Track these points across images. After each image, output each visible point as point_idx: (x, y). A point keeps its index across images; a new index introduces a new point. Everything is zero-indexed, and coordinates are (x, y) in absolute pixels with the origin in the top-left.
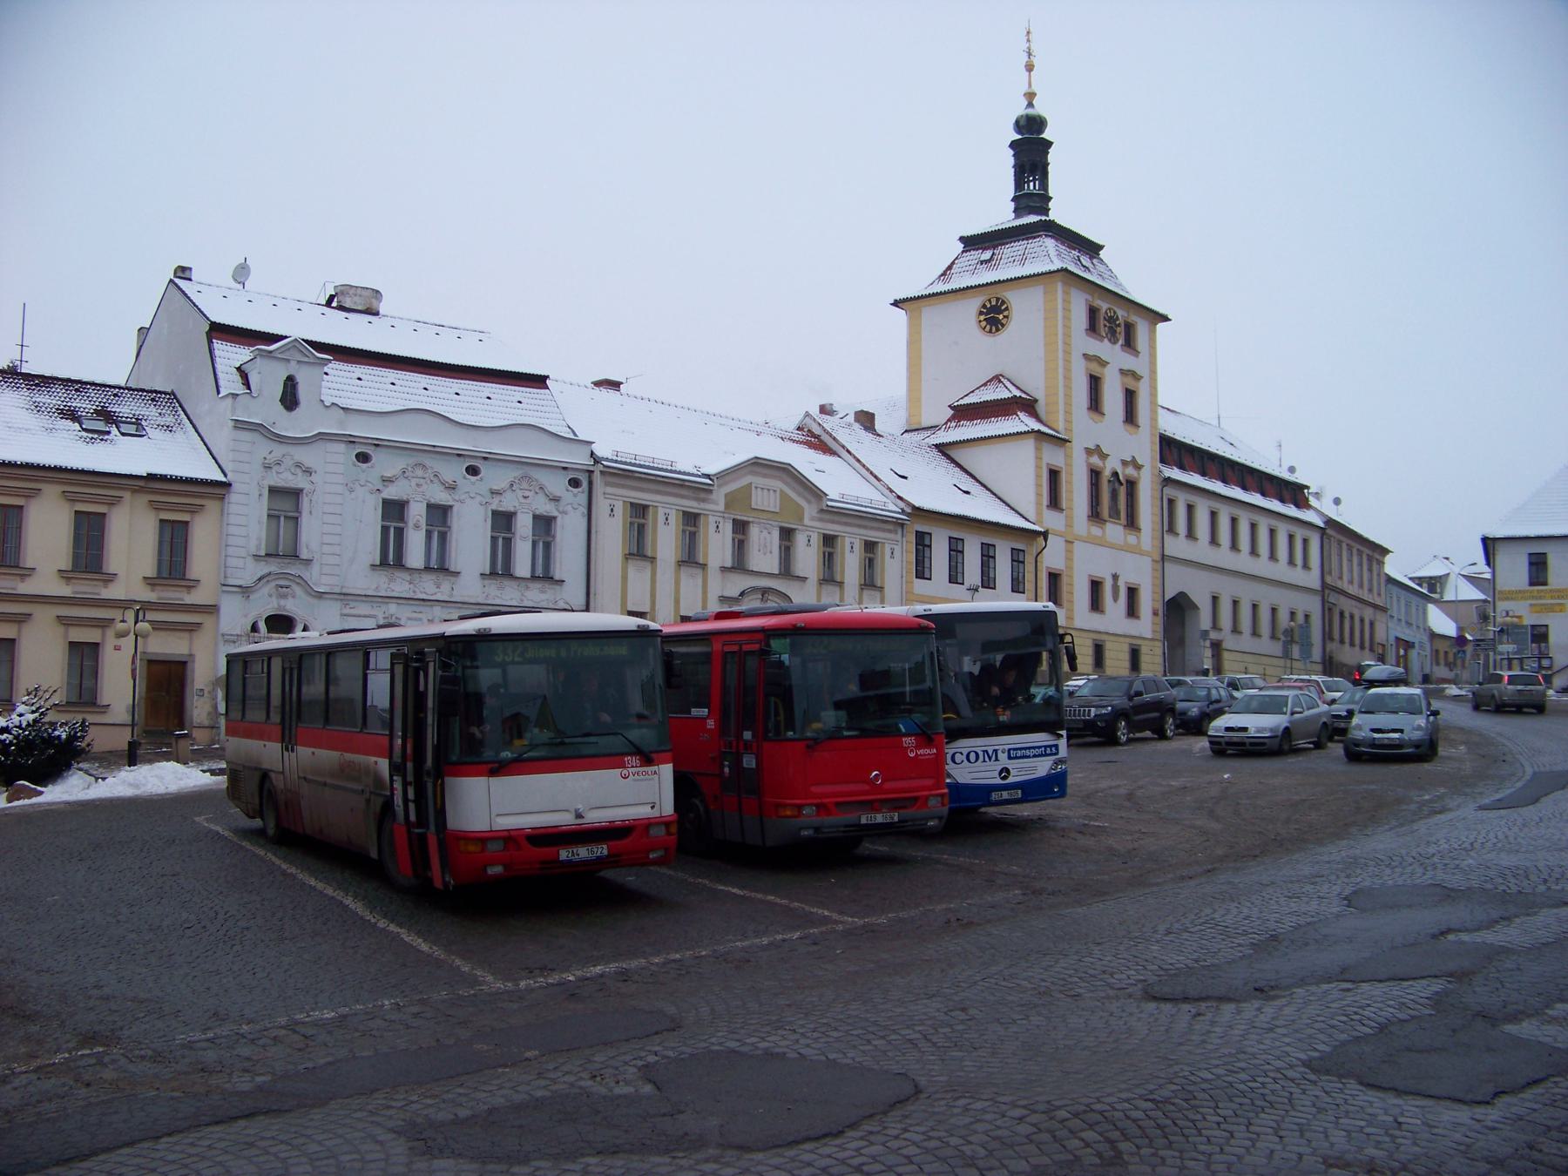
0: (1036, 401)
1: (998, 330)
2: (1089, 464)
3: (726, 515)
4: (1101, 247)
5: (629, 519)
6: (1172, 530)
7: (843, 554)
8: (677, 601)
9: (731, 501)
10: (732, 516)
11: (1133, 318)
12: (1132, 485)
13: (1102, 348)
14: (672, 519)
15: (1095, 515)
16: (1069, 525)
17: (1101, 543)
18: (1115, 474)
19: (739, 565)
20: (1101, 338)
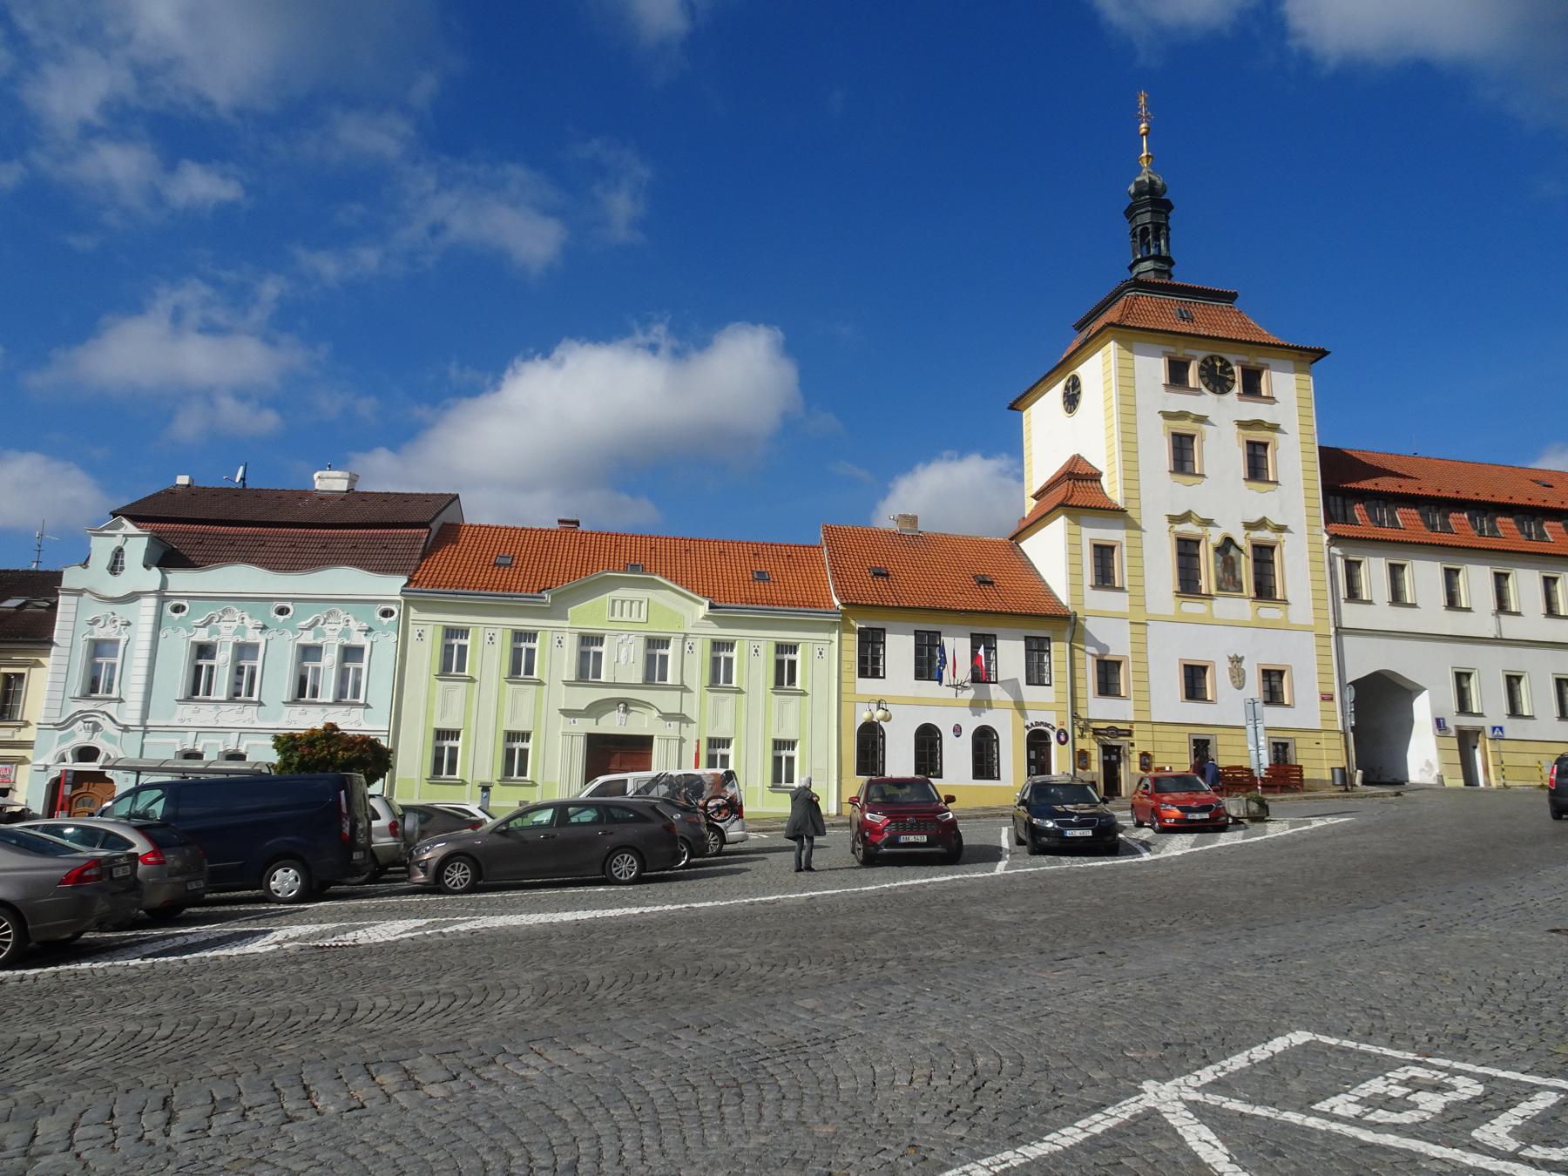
6: (1353, 595)
16: (1139, 602)
18: (1229, 541)
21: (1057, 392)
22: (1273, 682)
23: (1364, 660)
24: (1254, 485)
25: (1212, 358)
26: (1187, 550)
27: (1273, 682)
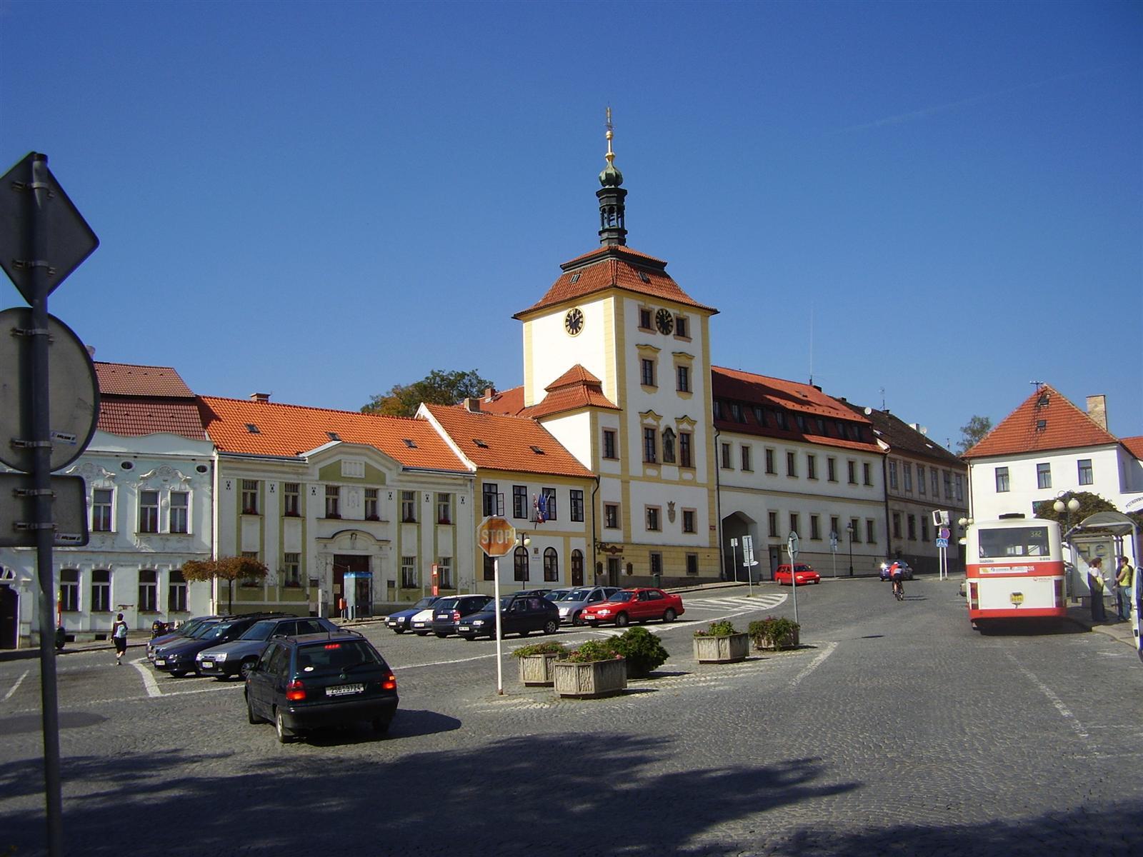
0: (601, 382)
1: (577, 332)
2: (642, 424)
3: (320, 483)
4: (665, 264)
5: (242, 491)
6: (727, 464)
7: (419, 503)
8: (282, 543)
9: (324, 474)
10: (326, 483)
11: (685, 313)
12: (686, 438)
13: (657, 339)
14: (277, 488)
15: (650, 459)
16: (625, 467)
17: (658, 480)
18: (669, 430)
19: (333, 515)
20: (654, 332)
21: (560, 317)
22: (689, 518)
23: (731, 504)
24: (682, 394)
25: (662, 310)
26: (649, 434)
27: (689, 518)
